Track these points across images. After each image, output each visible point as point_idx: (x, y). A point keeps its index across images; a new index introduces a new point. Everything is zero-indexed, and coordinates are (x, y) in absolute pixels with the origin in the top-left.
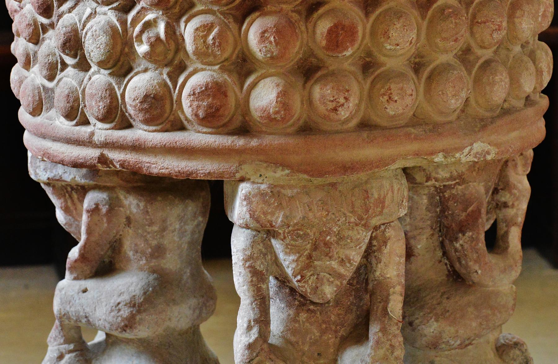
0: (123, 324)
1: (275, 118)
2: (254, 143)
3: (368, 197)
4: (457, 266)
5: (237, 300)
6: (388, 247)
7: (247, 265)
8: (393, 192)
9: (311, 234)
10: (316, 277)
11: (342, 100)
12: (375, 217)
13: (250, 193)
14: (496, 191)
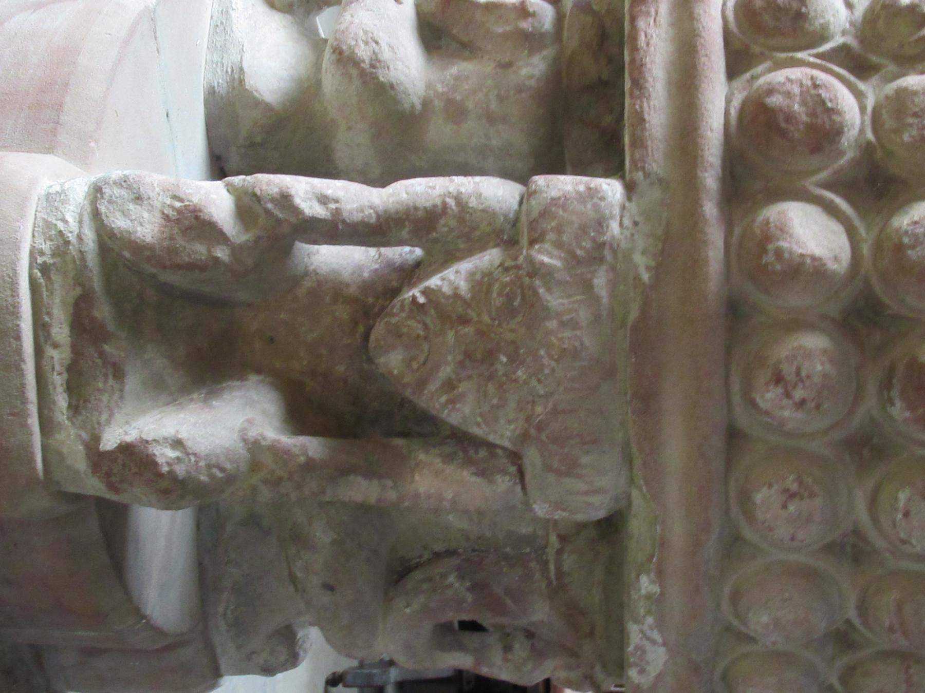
0: (344, 48)
1: (765, 251)
2: (710, 209)
3: (585, 443)
4: (417, 575)
5: (382, 182)
6: (474, 479)
7: (448, 200)
8: (587, 493)
9: (513, 324)
10: (422, 333)
11: (799, 394)
12: (542, 455)
13: (603, 199)
14: (530, 635)
